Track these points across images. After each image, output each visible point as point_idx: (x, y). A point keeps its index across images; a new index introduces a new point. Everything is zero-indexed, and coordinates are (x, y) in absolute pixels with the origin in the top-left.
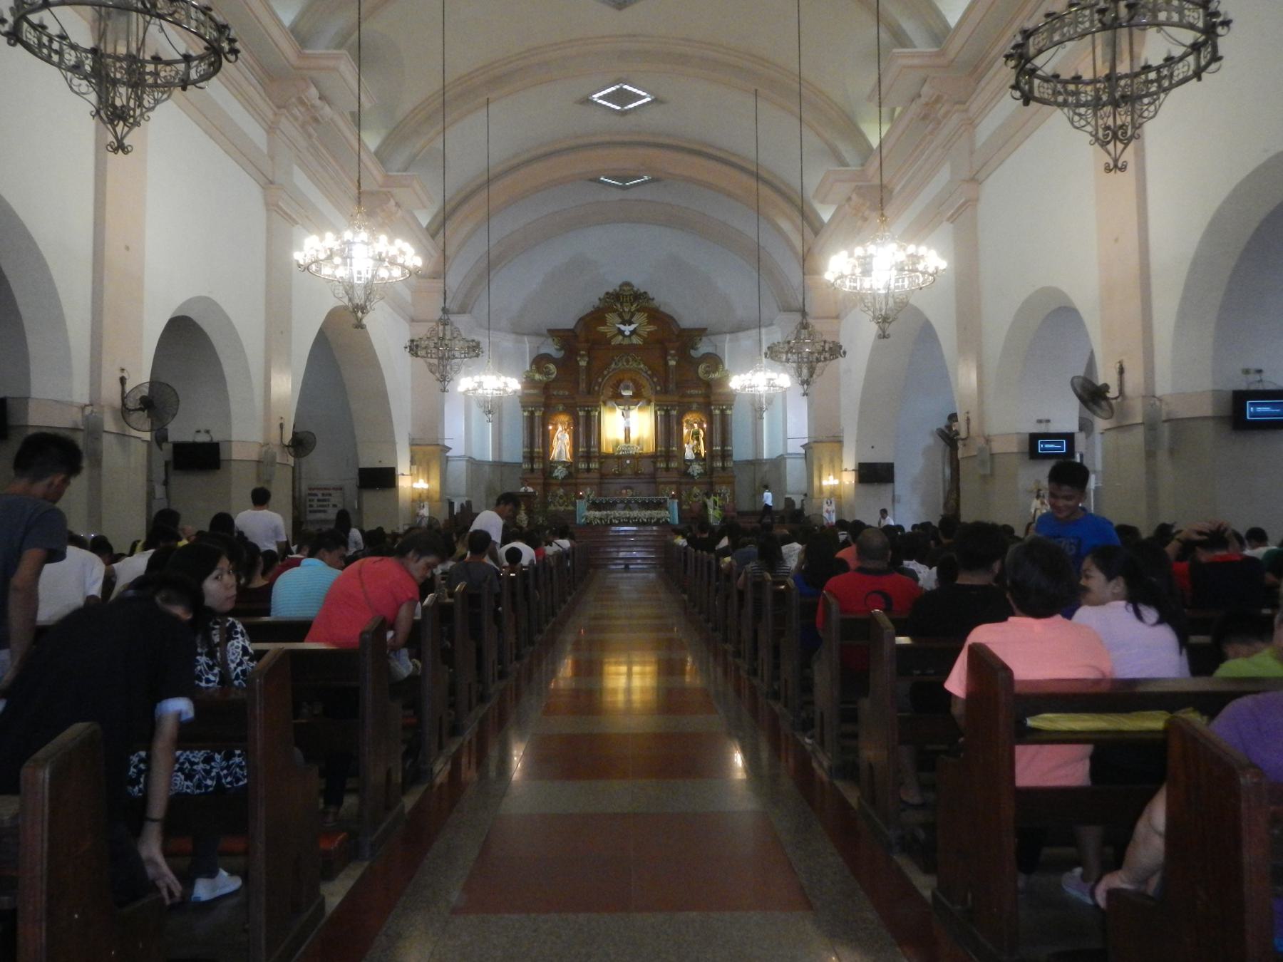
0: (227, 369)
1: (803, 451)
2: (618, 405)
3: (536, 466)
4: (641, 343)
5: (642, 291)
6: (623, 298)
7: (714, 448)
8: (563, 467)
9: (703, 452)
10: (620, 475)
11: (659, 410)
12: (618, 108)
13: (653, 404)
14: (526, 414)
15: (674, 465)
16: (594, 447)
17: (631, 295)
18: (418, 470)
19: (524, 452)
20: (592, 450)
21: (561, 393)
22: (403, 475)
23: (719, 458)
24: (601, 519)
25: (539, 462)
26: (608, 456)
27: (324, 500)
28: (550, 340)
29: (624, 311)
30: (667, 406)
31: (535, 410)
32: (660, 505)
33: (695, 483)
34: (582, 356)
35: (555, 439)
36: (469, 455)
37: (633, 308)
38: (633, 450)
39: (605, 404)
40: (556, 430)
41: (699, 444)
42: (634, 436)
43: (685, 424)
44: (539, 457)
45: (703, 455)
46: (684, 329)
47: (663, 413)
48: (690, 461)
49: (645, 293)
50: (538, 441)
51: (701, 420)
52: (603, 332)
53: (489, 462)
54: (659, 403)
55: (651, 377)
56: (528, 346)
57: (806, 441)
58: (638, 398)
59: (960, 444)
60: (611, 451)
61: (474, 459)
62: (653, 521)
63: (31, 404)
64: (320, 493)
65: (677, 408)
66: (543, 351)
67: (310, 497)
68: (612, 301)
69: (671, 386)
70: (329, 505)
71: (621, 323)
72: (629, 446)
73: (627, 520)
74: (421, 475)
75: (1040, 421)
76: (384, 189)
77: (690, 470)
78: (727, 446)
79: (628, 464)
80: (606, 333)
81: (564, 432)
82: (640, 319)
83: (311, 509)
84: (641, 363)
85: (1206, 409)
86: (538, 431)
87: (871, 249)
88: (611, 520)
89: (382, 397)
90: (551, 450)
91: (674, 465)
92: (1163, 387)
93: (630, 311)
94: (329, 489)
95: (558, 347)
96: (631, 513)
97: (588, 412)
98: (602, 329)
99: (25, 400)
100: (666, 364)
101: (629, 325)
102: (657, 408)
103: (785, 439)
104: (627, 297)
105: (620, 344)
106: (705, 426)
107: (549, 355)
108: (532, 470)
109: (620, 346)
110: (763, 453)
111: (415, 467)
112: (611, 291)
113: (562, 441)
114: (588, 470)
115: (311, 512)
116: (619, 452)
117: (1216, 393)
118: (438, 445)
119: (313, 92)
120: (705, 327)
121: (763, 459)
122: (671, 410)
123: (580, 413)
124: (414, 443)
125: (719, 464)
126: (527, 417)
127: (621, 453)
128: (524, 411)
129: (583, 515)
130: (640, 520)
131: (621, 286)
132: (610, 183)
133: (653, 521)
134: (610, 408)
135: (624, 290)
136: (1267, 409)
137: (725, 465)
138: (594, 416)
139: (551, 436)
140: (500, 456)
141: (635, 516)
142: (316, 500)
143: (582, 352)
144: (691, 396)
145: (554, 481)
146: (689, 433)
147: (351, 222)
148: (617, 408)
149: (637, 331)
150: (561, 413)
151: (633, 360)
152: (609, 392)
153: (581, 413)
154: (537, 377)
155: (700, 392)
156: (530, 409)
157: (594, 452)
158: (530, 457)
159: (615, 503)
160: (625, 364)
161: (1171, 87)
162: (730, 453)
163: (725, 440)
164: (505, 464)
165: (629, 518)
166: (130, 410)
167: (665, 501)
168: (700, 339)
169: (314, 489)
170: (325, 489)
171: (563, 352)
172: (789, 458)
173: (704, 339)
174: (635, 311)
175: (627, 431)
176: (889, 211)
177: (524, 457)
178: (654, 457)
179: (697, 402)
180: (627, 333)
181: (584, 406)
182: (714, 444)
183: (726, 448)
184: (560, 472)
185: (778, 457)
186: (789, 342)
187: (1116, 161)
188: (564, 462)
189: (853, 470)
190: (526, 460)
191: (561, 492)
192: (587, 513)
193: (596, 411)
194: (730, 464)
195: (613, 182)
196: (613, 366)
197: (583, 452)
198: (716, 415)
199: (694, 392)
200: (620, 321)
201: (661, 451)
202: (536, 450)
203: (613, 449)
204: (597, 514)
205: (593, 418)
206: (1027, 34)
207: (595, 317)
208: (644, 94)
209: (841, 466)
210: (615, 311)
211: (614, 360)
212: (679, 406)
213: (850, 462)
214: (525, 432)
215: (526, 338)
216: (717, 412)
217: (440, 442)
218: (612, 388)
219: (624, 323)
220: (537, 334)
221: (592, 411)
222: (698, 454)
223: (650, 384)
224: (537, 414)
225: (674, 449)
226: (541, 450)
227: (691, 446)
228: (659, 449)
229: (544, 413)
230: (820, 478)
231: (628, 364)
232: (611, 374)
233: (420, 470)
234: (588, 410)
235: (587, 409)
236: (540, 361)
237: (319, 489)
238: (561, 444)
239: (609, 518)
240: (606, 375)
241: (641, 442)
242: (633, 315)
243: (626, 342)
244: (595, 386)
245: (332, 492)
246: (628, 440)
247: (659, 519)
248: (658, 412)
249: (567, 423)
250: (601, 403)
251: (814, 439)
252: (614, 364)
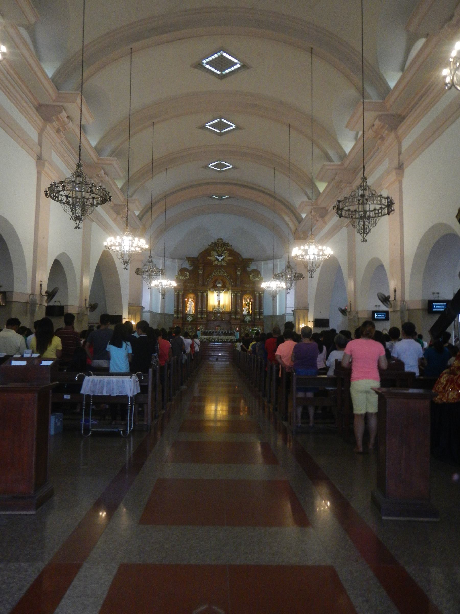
0: (69, 278)
1: (292, 313)
2: (215, 290)
3: (179, 316)
4: (226, 264)
5: (227, 242)
6: (219, 246)
7: (256, 310)
8: (191, 317)
9: (251, 312)
10: (215, 320)
11: (233, 293)
12: (219, 170)
13: (230, 290)
14: (176, 293)
15: (238, 317)
16: (204, 308)
17: (222, 243)
18: (131, 316)
19: (174, 310)
20: (203, 309)
21: (191, 285)
22: (125, 318)
23: (258, 314)
24: (207, 339)
25: (181, 314)
26: (210, 312)
28: (187, 262)
29: (219, 250)
30: (236, 292)
31: (180, 292)
32: (232, 334)
33: (247, 325)
34: (200, 269)
35: (188, 304)
36: (151, 311)
37: (223, 249)
38: (221, 310)
39: (210, 290)
40: (188, 300)
41: (249, 308)
42: (222, 304)
43: (244, 300)
44: (180, 312)
45: (251, 313)
46: (244, 259)
47: (234, 294)
48: (246, 315)
49: (228, 243)
50: (181, 305)
51: (250, 298)
52: (210, 259)
53: (160, 313)
54: (233, 290)
55: (230, 279)
56: (177, 264)
57: (294, 309)
58: (224, 288)
59: (348, 314)
60: (212, 310)
61: (153, 312)
62: (229, 341)
63: (14, 294)
65: (240, 293)
66: (184, 266)
68: (214, 246)
69: (238, 283)
71: (217, 256)
72: (219, 308)
73: (218, 340)
74: (132, 319)
75: (376, 306)
76: (123, 204)
77: (245, 319)
78: (261, 309)
79: (219, 316)
80: (211, 260)
81: (192, 301)
82: (226, 254)
84: (226, 273)
85: (419, 306)
86: (181, 301)
87: (306, 247)
88: (211, 340)
89: (117, 286)
90: (186, 309)
91: (238, 317)
92: (407, 298)
93: (221, 250)
94: (93, 323)
95: (190, 265)
96: (220, 337)
97: (202, 293)
98: (209, 258)
99: (12, 292)
100: (236, 273)
101: (221, 257)
102: (232, 292)
103: (286, 308)
104: (220, 245)
105: (217, 264)
106: (252, 300)
107: (186, 268)
108: (178, 317)
109: (217, 266)
110: (276, 312)
111: (130, 316)
113: (191, 305)
114: (202, 318)
116: (215, 310)
117: (422, 300)
118: (140, 306)
119: (103, 172)
120: (252, 258)
121: (277, 315)
122: (238, 293)
123: (199, 294)
124: (130, 305)
125: (258, 317)
126: (176, 294)
127: (216, 311)
128: (175, 292)
129: (200, 337)
130: (223, 340)
131: (217, 240)
132: (214, 197)
133: (229, 341)
134: (212, 291)
135: (219, 242)
136: (380, 315)
137: (260, 317)
138: (205, 295)
139: (186, 303)
140: (164, 311)
141: (221, 338)
143: (201, 268)
144: (247, 287)
145: (187, 323)
146: (245, 303)
147: (124, 231)
148: (215, 292)
149: (224, 259)
150: (190, 293)
151: (222, 271)
152: (212, 285)
153: (199, 294)
154: (181, 277)
155: (250, 286)
156: (178, 291)
157: (205, 310)
158: (177, 312)
159: (213, 333)
160: (219, 273)
161: (382, 216)
162: (263, 312)
163: (260, 307)
164: (166, 314)
165: (219, 339)
166: (43, 296)
167: (234, 332)
168: (251, 263)
171: (192, 268)
172: (288, 315)
173: (253, 263)
174: (223, 250)
175: (219, 302)
176: (326, 219)
177: (174, 312)
178: (230, 313)
180: (220, 260)
181: (201, 291)
182: (256, 309)
183: (261, 310)
184: (190, 319)
185: (283, 314)
186: (282, 273)
187: (364, 239)
188: (191, 314)
189: (312, 322)
190: (175, 313)
191: (190, 327)
192: (201, 337)
193: (206, 293)
194: (262, 317)
195: (216, 197)
196: (214, 274)
197: (199, 310)
198: (257, 296)
199: (247, 286)
200: (217, 254)
201: (233, 311)
202: (180, 309)
203: (213, 310)
204: (206, 337)
205: (204, 296)
206: (339, 201)
207: (206, 253)
208: (229, 165)
209: (308, 320)
210: (215, 250)
211: (214, 271)
212: (241, 292)
213: (311, 318)
214: (175, 301)
215: (176, 261)
216: (258, 295)
217: (140, 305)
218: (213, 283)
219: (219, 255)
220: (181, 259)
221: (204, 293)
222: (249, 312)
223: (229, 282)
224: (180, 293)
225: (239, 310)
226: (182, 309)
227: (246, 309)
228: (232, 310)
229: (184, 293)
230: (299, 325)
231: (220, 273)
232: (212, 278)
233: (132, 316)
234: (202, 293)
235: (202, 292)
236: (182, 271)
238: (191, 307)
239: (210, 339)
241: (224, 307)
242: (222, 252)
243: (219, 264)
246: (219, 305)
247: (231, 340)
248: (232, 294)
249: (193, 298)
250: (208, 289)
251: (296, 308)
252: (214, 273)
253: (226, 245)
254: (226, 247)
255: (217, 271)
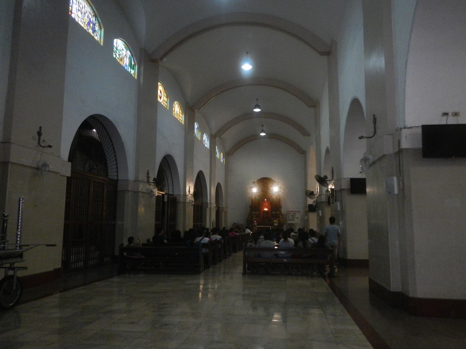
27: (293, 216)
64: (292, 213)
67: (288, 215)
70: (295, 218)
83: (289, 219)
94: (295, 212)
115: (289, 220)
142: (290, 216)
169: (289, 212)
170: (294, 212)
237: (292, 212)
245: (296, 213)
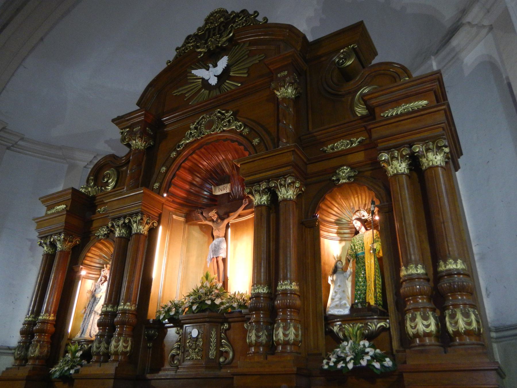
7: (403, 273)
44: (41, 332)
49: (244, 12)
101: (215, 66)
112: (193, 31)
131: (207, 21)
179: (348, 166)
180: (213, 81)
181: (119, 218)
183: (442, 268)
199: (341, 145)
240: (175, 159)
244: (155, 182)
253: (234, 23)
254: (236, 26)
255: (201, 124)
